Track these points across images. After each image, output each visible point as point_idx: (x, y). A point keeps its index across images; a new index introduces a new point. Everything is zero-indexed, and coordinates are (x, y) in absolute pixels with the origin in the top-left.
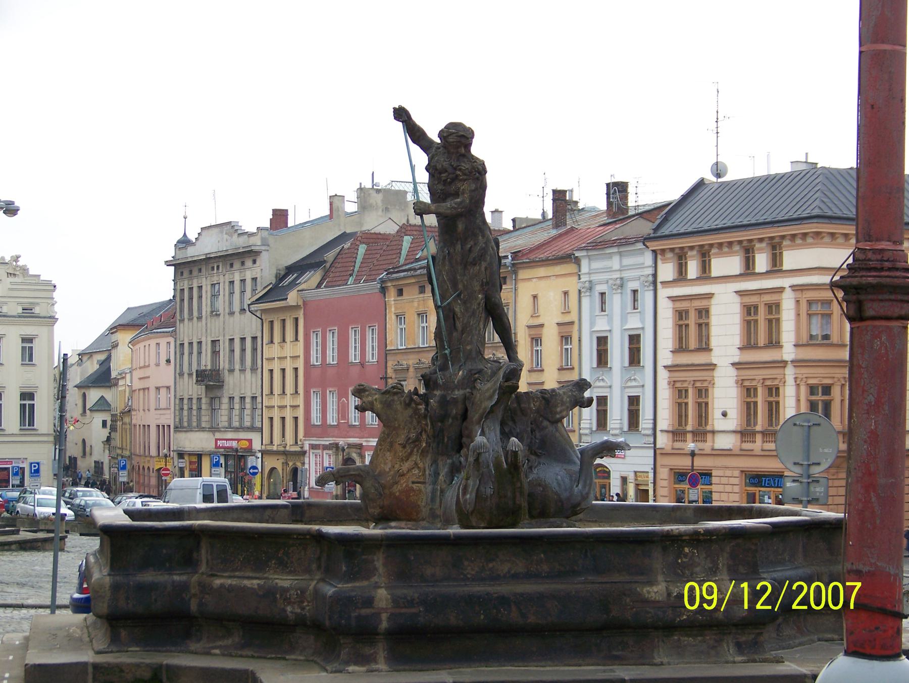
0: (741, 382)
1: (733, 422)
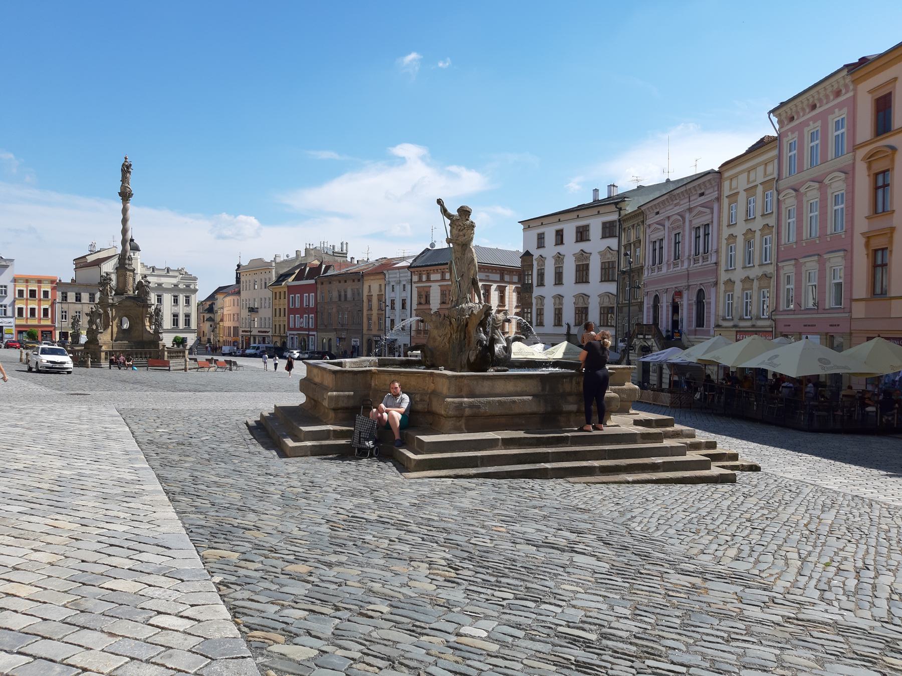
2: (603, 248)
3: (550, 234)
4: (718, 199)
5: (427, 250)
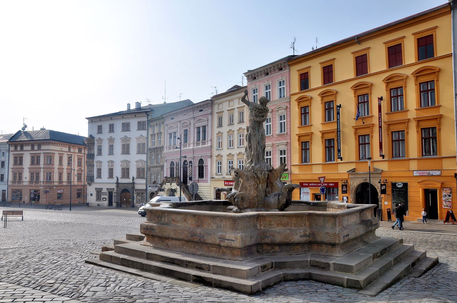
0: (30, 172)
1: (28, 179)
4: (212, 114)
5: (20, 131)
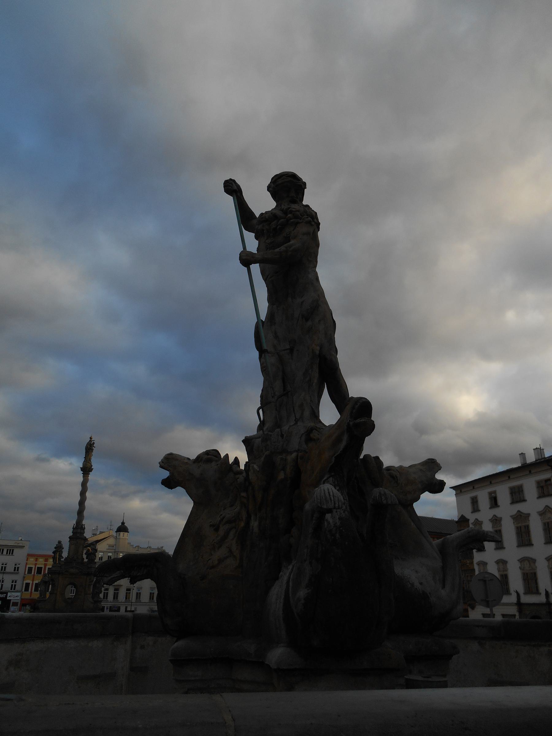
2: (541, 508)
3: (483, 496)
